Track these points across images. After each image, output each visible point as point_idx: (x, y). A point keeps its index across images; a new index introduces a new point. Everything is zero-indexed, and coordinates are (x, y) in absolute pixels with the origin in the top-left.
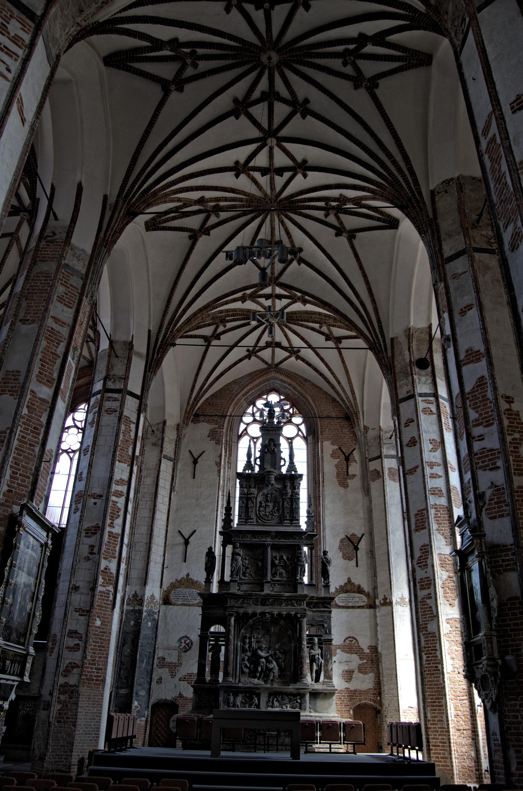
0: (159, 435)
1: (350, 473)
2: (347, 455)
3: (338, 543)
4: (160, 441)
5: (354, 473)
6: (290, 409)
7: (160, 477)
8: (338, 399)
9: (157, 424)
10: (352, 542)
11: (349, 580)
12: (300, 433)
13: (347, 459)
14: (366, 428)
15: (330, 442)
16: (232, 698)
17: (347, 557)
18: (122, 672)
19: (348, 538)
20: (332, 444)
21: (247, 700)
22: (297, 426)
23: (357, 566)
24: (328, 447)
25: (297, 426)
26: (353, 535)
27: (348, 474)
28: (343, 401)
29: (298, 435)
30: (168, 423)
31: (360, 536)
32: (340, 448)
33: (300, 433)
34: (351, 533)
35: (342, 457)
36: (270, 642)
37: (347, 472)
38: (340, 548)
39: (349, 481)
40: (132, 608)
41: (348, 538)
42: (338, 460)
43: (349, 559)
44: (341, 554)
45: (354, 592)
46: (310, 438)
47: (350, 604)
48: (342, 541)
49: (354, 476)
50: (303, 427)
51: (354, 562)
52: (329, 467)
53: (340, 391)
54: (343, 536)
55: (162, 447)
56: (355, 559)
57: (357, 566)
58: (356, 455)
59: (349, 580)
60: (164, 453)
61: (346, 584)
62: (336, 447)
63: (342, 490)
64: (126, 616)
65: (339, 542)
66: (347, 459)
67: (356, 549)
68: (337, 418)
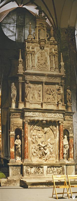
21: (37, 170)
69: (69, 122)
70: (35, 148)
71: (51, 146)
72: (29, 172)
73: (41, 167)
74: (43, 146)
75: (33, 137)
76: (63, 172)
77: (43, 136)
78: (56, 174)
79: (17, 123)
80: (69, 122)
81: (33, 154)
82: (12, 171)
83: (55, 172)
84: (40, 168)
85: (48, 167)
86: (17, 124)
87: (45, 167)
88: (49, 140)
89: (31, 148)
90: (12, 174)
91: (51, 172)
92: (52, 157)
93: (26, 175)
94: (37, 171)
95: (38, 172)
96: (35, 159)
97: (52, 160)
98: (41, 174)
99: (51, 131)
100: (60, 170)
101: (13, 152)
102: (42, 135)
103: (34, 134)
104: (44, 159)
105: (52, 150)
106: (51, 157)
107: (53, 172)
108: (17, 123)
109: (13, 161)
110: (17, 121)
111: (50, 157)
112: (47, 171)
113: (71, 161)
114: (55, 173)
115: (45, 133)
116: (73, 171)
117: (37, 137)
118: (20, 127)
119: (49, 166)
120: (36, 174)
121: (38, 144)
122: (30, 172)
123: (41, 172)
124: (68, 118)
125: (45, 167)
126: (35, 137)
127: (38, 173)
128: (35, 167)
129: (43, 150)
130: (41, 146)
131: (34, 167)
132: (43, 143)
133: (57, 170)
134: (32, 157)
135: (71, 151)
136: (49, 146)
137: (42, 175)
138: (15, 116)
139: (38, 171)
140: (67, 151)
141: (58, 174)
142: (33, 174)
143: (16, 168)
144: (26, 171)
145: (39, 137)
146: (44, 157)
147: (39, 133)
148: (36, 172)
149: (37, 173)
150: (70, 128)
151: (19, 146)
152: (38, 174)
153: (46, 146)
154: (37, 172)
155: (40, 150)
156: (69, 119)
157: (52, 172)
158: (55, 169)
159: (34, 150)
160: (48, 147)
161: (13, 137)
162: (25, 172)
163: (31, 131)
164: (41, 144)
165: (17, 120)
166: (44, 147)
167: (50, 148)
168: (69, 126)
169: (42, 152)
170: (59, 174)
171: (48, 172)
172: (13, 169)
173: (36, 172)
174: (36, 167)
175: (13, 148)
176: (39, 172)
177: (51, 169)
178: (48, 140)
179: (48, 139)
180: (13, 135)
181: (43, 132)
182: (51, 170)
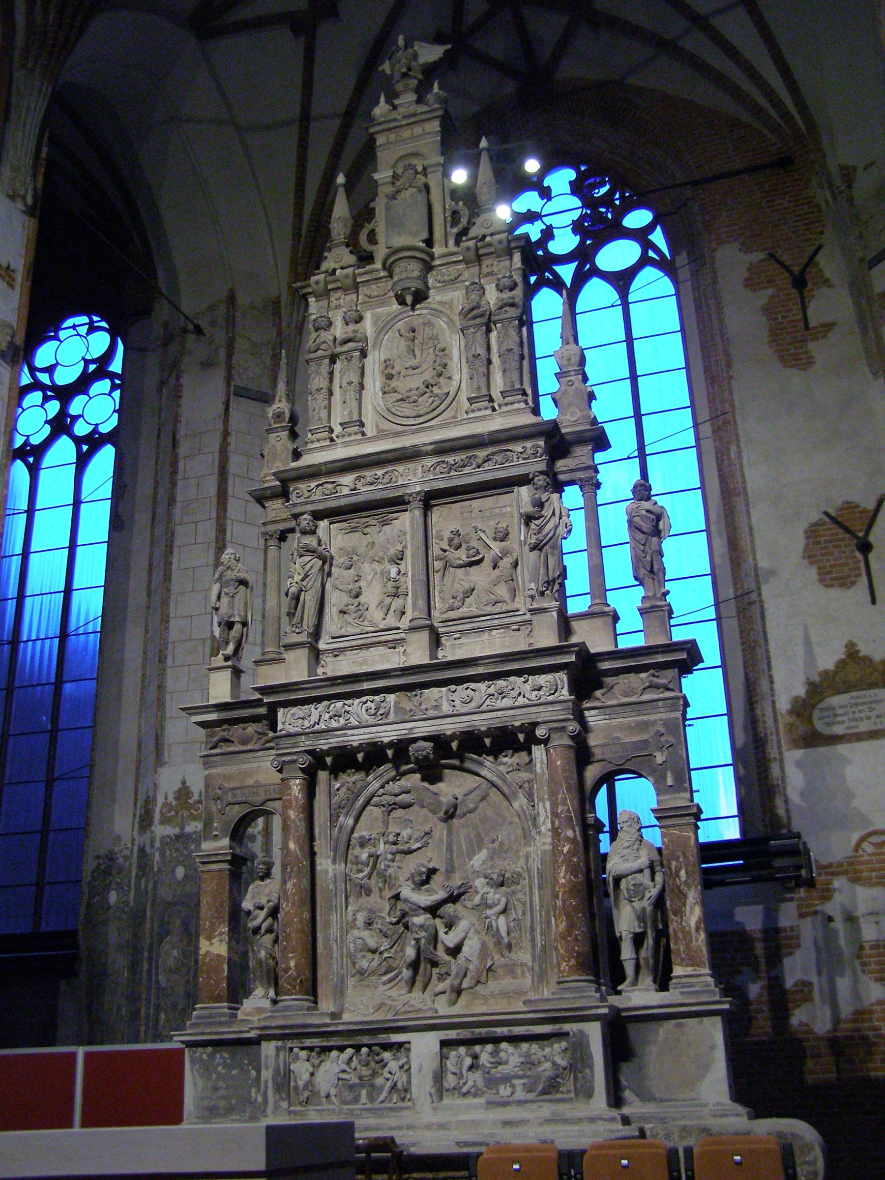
0: (220, 337)
1: (814, 320)
2: (796, 270)
3: (799, 543)
4: (222, 353)
5: (827, 319)
6: (610, 194)
7: (231, 448)
8: (746, 117)
9: (212, 308)
10: (847, 530)
11: (852, 653)
12: (651, 254)
13: (800, 282)
14: (848, 173)
15: (737, 245)
16: (301, 1069)
17: (834, 578)
18: (163, 1016)
19: (833, 519)
20: (746, 249)
21: (365, 1072)
22: (641, 236)
23: (874, 602)
24: (732, 261)
25: (641, 236)
26: (849, 506)
27: (807, 327)
28: (757, 111)
29: (643, 262)
30: (241, 300)
31: (871, 505)
32: (772, 256)
33: (651, 254)
34: (839, 502)
35: (783, 280)
36: (450, 849)
37: (805, 319)
38: (809, 556)
39: (812, 346)
40: (177, 831)
41: (833, 519)
42: (770, 291)
43: (845, 582)
44: (813, 573)
45: (872, 686)
46: (682, 259)
47: (864, 727)
48: (812, 532)
49: (829, 327)
50: (658, 237)
51: (861, 589)
52: (745, 316)
53: (748, 86)
54: (815, 516)
55: (229, 368)
56: (864, 579)
57: (874, 602)
58: (830, 264)
59: (852, 653)
60: (237, 382)
61: (841, 665)
62: (761, 255)
63: (795, 378)
64: (163, 854)
65: (801, 534)
66: (800, 282)
67: (865, 547)
68: (752, 169)
69: (645, 718)
70: (369, 924)
71: (493, 895)
72: (301, 1084)
73: (386, 1047)
74: (424, 899)
75: (357, 851)
76: (576, 1079)
77: (436, 835)
78: (520, 1094)
79: (250, 782)
80: (645, 718)
81: (354, 963)
82: (200, 1083)
83: (507, 1079)
84: (387, 1055)
85: (444, 1043)
86: (246, 791)
87: (424, 1046)
88: (478, 860)
89: (349, 930)
90: (205, 1103)
91: (470, 1083)
92: (511, 970)
93: (277, 1107)
94: (361, 1078)
95: (373, 1086)
96: (369, 993)
97: (504, 994)
98: (395, 1097)
99: (494, 795)
100: (548, 1065)
101: (219, 956)
102: (427, 829)
103: (366, 834)
104: (441, 987)
105: (502, 923)
106: (500, 971)
107: (492, 1082)
108: (248, 787)
109: (211, 1016)
110: (246, 774)
111: (490, 969)
112: (439, 1077)
113: (677, 991)
114: (504, 1091)
115: (450, 815)
116: (704, 1067)
117: (382, 848)
118: (269, 803)
119: (452, 1034)
120: (356, 1100)
121: (393, 893)
122: (306, 1086)
123: (389, 1083)
124: (632, 692)
125: (424, 1046)
126: (373, 850)
127: (374, 1091)
128: (350, 1051)
129: (421, 927)
130: (406, 900)
131: (342, 1049)
132: (437, 879)
133: (529, 1063)
134: (351, 982)
135: (680, 913)
136: (477, 899)
137: (407, 1104)
138: (231, 749)
139: (374, 1074)
140: (641, 917)
141: (531, 1096)
142: (328, 1096)
143: (233, 1058)
144: (273, 1078)
145: (405, 847)
146: (441, 978)
147: (407, 823)
148: (357, 1081)
149: (364, 1092)
150: (660, 758)
151: (255, 918)
152: (371, 1098)
153: (453, 899)
154: (362, 1086)
155: (406, 927)
156: (646, 697)
157: (480, 1083)
158: (512, 1055)
159: (365, 934)
160: (469, 904)
161: (220, 870)
162: (270, 1084)
163: (341, 819)
164: (406, 892)
165: (245, 766)
166: (433, 910)
167: (489, 912)
168: (646, 742)
169: (417, 940)
170: (544, 1092)
171: (450, 1081)
172: (207, 1069)
173: (351, 1087)
174: (358, 1048)
175: (222, 933)
176: (379, 1081)
177: (476, 1057)
178: (470, 859)
179: (471, 853)
180: (220, 858)
181: (434, 812)
182: (471, 1068)
